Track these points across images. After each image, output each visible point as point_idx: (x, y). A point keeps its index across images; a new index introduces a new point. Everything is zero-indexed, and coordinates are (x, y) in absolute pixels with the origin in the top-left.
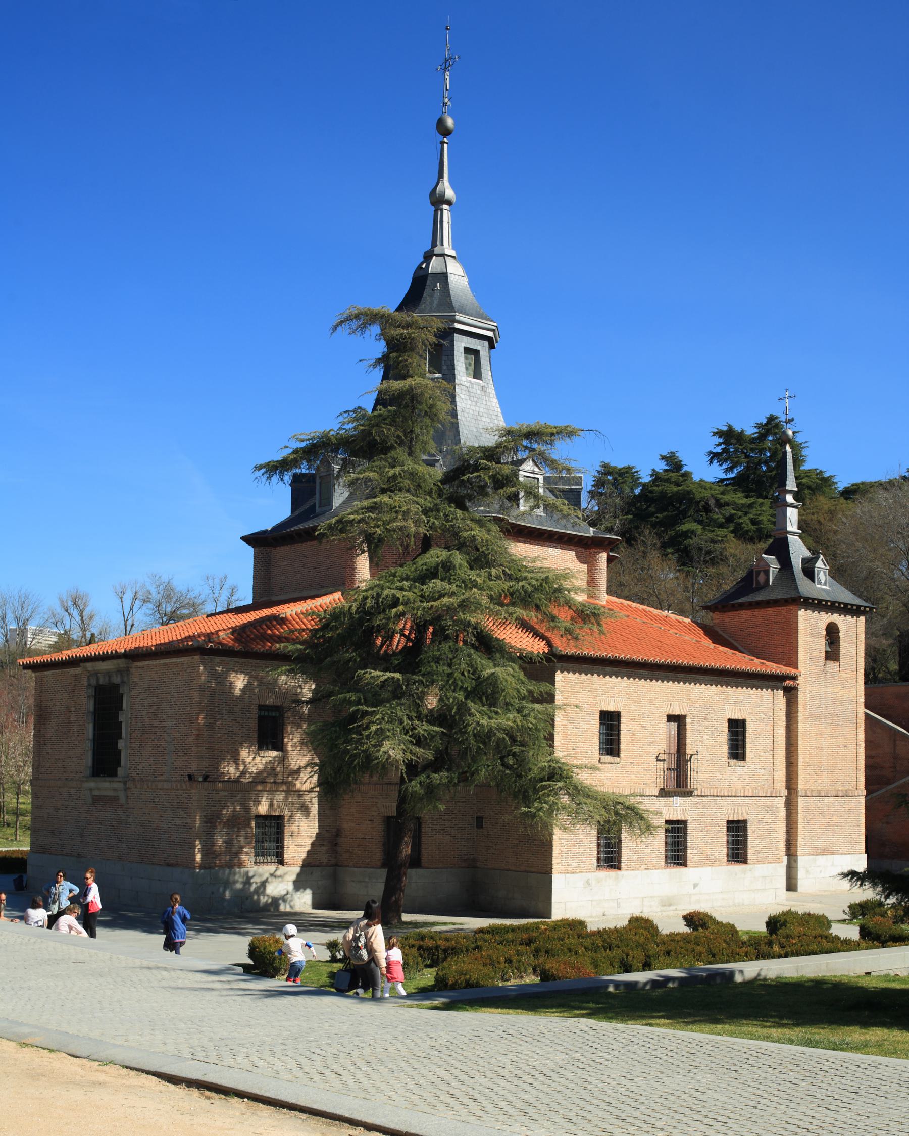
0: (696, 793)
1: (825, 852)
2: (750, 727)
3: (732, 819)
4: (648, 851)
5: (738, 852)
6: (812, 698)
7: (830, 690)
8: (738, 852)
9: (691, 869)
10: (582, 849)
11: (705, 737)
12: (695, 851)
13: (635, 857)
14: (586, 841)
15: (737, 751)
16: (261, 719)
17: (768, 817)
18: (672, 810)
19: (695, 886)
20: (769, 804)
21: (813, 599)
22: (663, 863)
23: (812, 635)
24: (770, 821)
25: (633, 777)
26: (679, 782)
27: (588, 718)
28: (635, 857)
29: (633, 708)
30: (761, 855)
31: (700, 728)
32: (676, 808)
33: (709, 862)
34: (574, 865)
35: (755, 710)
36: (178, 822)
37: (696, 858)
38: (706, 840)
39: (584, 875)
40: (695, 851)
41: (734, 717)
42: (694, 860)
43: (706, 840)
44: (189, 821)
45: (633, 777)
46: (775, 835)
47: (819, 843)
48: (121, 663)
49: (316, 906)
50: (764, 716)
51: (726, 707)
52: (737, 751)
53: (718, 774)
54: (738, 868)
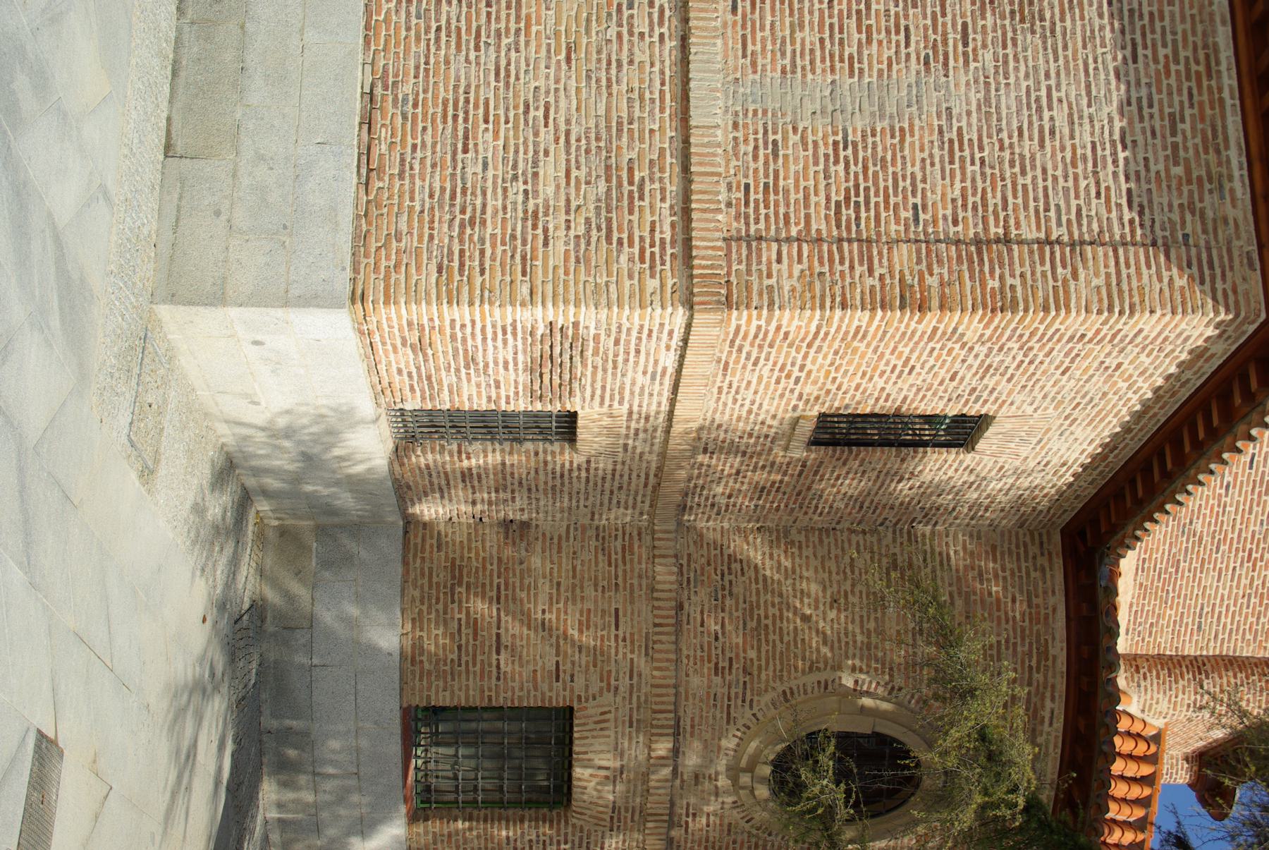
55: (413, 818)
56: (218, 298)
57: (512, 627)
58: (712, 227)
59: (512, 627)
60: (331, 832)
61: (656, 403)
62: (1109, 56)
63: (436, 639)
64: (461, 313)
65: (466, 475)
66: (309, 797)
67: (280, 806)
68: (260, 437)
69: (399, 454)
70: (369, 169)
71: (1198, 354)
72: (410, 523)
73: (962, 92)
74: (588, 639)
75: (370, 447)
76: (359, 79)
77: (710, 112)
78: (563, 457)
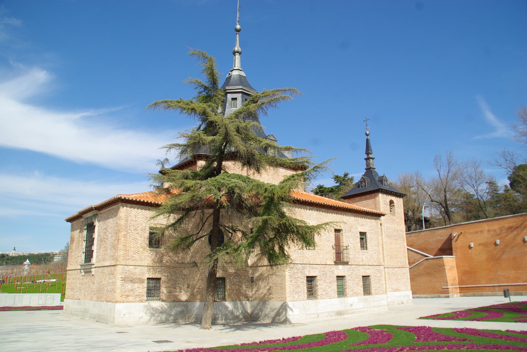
0: (349, 263)
1: (397, 290)
2: (368, 235)
3: (364, 275)
4: (329, 290)
6: (387, 229)
7: (393, 226)
9: (349, 298)
10: (300, 289)
11: (351, 239)
13: (324, 293)
14: (302, 286)
16: (151, 234)
18: (339, 271)
19: (351, 305)
21: (385, 190)
22: (337, 296)
23: (385, 204)
25: (321, 256)
26: (339, 260)
28: (324, 293)
32: (341, 270)
33: (357, 294)
34: (297, 297)
36: (111, 281)
37: (351, 293)
38: (354, 285)
39: (301, 302)
41: (362, 231)
43: (354, 285)
44: (114, 280)
45: (321, 256)
46: (381, 282)
47: (394, 287)
48: (95, 212)
51: (358, 227)
54: (368, 297)
55: (226, 301)
56: (114, 317)
57: (197, 286)
58: (113, 263)
59: (197, 286)
60: (227, 312)
61: (146, 268)
62: (108, 220)
63: (199, 297)
64: (118, 291)
65: (170, 292)
66: (220, 316)
67: (222, 320)
68: (153, 318)
69: (163, 301)
70: (109, 301)
71: (131, 208)
72: (186, 301)
73: (109, 236)
74: (199, 276)
75: (157, 304)
76: (105, 302)
77: (107, 264)
78: (163, 278)
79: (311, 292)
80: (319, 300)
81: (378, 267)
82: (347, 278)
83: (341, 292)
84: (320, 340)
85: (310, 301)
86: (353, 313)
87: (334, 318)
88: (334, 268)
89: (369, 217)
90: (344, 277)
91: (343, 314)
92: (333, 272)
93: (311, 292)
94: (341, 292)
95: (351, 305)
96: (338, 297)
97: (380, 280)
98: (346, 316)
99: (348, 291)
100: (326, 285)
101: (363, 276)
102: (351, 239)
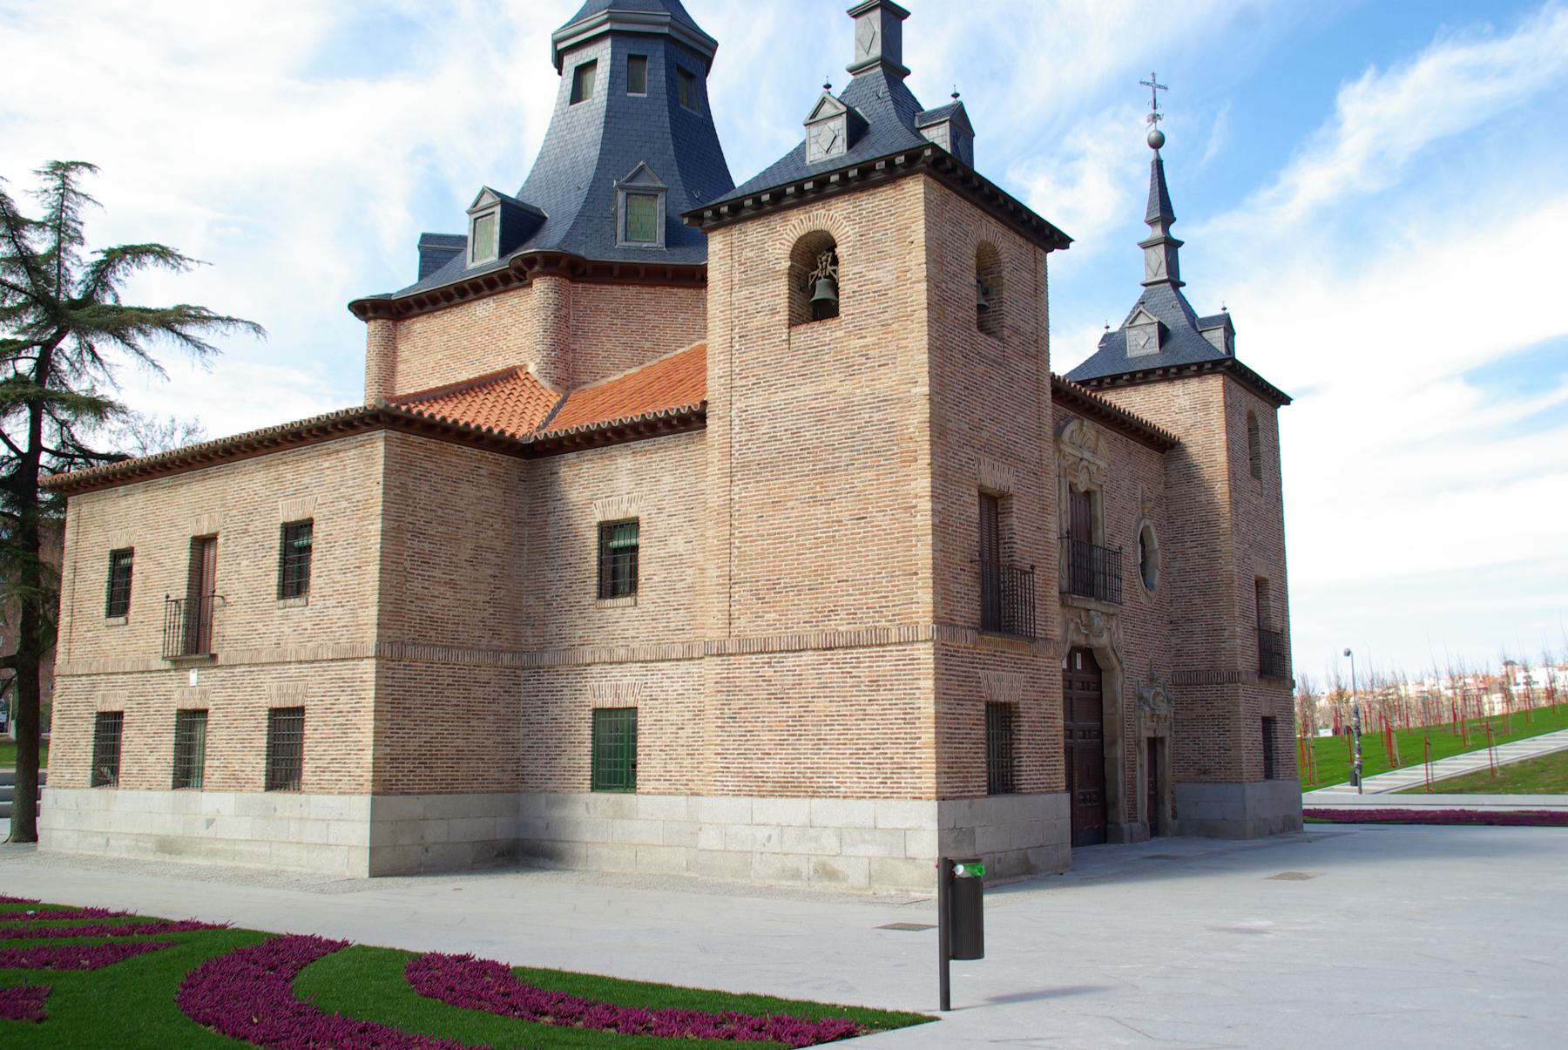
0: (221, 660)
4: (152, 759)
5: (283, 771)
8: (283, 771)
11: (245, 563)
12: (217, 763)
14: (83, 743)
15: (294, 577)
17: (345, 702)
19: (210, 823)
20: (347, 674)
22: (170, 782)
24: (346, 708)
25: (142, 643)
27: (97, 566)
28: (135, 770)
29: (150, 537)
30: (327, 776)
31: (237, 549)
33: (235, 782)
34: (68, 776)
35: (330, 497)
37: (217, 776)
40: (217, 763)
42: (214, 778)
43: (237, 746)
46: (356, 736)
49: (394, 858)
50: (345, 504)
52: (294, 577)
53: (260, 625)
79: (106, 768)
80: (119, 793)
81: (345, 670)
82: (213, 718)
83: (186, 773)
84: (248, 947)
85: (95, 791)
86: (213, 853)
87: (150, 857)
88: (172, 682)
89: (332, 445)
90: (205, 712)
91: (180, 853)
92: (167, 697)
93: (106, 768)
94: (186, 773)
95: (210, 823)
96: (175, 787)
97: (345, 729)
98: (186, 860)
99: (212, 766)
100: (148, 747)
101: (274, 713)
102: (245, 563)
